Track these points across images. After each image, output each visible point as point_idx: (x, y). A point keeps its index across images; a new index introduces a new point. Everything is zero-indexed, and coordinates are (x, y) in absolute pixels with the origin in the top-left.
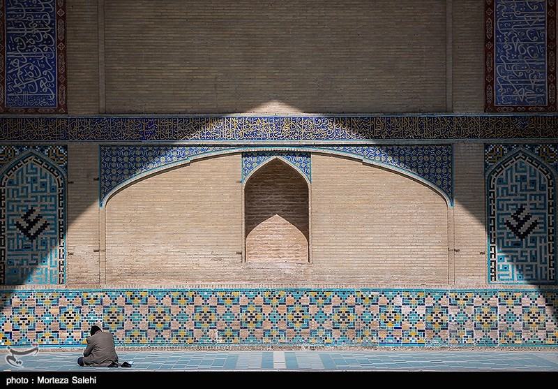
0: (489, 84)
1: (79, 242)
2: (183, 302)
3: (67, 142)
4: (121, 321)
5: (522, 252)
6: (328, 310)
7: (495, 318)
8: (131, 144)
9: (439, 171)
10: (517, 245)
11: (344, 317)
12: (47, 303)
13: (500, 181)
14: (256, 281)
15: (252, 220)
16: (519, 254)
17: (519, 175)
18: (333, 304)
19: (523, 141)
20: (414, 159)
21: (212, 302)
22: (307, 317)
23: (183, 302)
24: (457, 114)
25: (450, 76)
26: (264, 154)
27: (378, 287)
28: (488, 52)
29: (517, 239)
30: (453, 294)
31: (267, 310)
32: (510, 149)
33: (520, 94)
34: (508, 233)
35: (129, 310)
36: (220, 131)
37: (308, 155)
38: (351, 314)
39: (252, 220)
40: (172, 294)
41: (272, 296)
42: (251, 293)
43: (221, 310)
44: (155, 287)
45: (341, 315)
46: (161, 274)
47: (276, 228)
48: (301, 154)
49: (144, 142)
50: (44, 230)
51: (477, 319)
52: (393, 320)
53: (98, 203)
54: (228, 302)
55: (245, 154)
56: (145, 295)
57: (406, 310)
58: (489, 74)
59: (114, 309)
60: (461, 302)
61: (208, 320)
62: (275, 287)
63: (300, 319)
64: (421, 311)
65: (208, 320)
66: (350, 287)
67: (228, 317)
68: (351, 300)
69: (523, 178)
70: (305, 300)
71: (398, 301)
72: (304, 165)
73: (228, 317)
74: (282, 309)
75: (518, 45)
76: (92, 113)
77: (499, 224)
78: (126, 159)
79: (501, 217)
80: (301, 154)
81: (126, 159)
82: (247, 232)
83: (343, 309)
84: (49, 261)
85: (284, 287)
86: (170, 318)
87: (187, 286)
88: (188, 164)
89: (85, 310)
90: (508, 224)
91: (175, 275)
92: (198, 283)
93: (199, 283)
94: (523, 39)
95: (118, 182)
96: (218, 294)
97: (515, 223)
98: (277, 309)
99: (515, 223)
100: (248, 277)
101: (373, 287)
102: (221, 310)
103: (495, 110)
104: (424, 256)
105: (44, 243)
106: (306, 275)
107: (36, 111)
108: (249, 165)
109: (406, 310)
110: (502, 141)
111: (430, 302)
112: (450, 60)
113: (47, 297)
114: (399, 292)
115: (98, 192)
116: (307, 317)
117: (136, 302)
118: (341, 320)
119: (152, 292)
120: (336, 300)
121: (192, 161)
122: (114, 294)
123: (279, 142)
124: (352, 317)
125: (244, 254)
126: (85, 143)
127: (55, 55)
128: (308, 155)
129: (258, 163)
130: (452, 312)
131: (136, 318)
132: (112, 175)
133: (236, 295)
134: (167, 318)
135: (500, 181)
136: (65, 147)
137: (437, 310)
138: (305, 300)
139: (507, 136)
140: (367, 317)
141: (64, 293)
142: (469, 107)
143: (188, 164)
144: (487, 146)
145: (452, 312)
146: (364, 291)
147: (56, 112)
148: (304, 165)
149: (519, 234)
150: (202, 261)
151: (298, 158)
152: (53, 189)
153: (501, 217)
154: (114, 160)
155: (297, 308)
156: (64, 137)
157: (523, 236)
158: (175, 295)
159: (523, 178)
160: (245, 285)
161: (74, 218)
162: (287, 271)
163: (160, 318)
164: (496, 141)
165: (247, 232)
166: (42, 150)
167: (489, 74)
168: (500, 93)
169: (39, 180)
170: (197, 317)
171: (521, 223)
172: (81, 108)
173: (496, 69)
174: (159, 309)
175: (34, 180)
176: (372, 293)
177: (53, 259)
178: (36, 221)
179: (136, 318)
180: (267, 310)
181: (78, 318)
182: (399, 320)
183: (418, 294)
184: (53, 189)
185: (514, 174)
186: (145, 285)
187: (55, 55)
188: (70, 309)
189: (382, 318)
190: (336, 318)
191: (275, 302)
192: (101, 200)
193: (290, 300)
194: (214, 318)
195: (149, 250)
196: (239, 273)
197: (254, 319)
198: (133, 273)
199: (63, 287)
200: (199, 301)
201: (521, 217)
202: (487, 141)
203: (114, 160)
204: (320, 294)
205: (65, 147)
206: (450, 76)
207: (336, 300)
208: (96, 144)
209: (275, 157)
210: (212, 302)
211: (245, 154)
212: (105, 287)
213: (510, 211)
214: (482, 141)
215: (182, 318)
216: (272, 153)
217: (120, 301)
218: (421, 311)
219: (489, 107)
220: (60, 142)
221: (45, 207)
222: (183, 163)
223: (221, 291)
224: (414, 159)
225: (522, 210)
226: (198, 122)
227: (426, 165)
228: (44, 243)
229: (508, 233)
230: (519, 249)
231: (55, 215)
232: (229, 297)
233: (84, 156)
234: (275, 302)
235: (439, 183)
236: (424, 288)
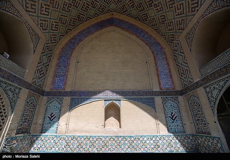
0: (160, 84)
1: (62, 121)
2: (87, 139)
3: (63, 97)
4: (69, 145)
5: (175, 124)
6: (126, 142)
7: (172, 143)
8: (78, 98)
9: (151, 104)
10: (173, 122)
11: (131, 144)
12: (51, 139)
13: (166, 106)
14: (107, 133)
15: (107, 117)
16: (174, 125)
17: (170, 104)
18: (128, 140)
19: (170, 96)
20: (145, 101)
21: (95, 140)
22: (121, 144)
23: (87, 139)
24: (154, 90)
25: (151, 83)
26: (109, 100)
27: (140, 135)
28: (158, 78)
29: (173, 121)
30: (160, 137)
31: (110, 142)
32: (167, 98)
33: (167, 86)
34: (170, 119)
35: (72, 142)
36: (101, 95)
37: (120, 100)
38: (133, 143)
39: (107, 117)
40: (84, 137)
41: (111, 138)
42: (105, 137)
43: (97, 142)
44: (80, 135)
45: (130, 143)
46: (82, 131)
47: (112, 120)
48: (118, 100)
49: (81, 97)
50: (53, 119)
51: (167, 144)
52: (144, 145)
53: (68, 112)
54: (99, 140)
55: (105, 100)
56: (77, 137)
57: (148, 142)
58: (159, 82)
59: (68, 141)
60: (162, 139)
61: (93, 145)
62: (112, 135)
63: (119, 145)
64: (152, 142)
65: (93, 145)
66: (132, 135)
67: (99, 144)
68: (133, 139)
69: (171, 105)
70: (120, 139)
71: (145, 139)
72: (119, 103)
73: (99, 144)
74: (114, 142)
75: (164, 76)
76: (70, 90)
77: (168, 117)
78: (76, 101)
79: (168, 115)
80: (118, 100)
81: (76, 101)
82: (105, 120)
83: (131, 142)
84: (54, 127)
85: (114, 135)
86: (83, 144)
87: (88, 135)
88: (91, 102)
89: (60, 141)
90: (170, 117)
91: (86, 132)
92: (92, 134)
93: (92, 134)
94: (165, 75)
95: (74, 107)
96: (96, 137)
97: (171, 117)
98: (112, 142)
99: (171, 117)
100: (105, 132)
101: (138, 135)
102: (97, 142)
103: (162, 90)
104: (150, 126)
105: (54, 122)
106: (120, 132)
107: (58, 90)
108: (106, 103)
109: (148, 142)
110: (165, 96)
111: (154, 139)
112: (151, 80)
113: (51, 137)
114: (145, 136)
115: (69, 109)
116: (121, 144)
117: (74, 139)
118: (130, 145)
119: (79, 136)
120: (129, 139)
121: (92, 102)
122: (69, 137)
123: (113, 97)
124: (133, 144)
125: (105, 126)
126: (67, 97)
127: (65, 78)
128: (120, 100)
129: (108, 102)
130: (160, 142)
131: (74, 144)
132: (72, 106)
133: (101, 137)
134: (82, 144)
135: (166, 106)
136: (63, 98)
137: (156, 142)
138: (120, 139)
139: (166, 95)
140: (137, 144)
141: (56, 136)
142: (157, 89)
143: (91, 102)
144: (162, 98)
145: (160, 142)
146: (136, 136)
147: (63, 90)
148: (119, 103)
149: (173, 119)
150: (93, 128)
151: (117, 101)
152: (59, 108)
153: (168, 115)
154: (74, 101)
155: (118, 141)
156: (63, 95)
157: (174, 120)
158: (85, 137)
159: (171, 105)
160: (104, 135)
161: (62, 115)
162: (115, 131)
163: (80, 144)
164: (164, 97)
165: (105, 120)
166: (58, 99)
167: (159, 82)
168: (162, 86)
169: (56, 106)
170: (91, 144)
171: (173, 117)
172: (68, 89)
173: (161, 81)
174: (80, 142)
175: (55, 106)
176: (138, 137)
177: (55, 126)
178: (53, 116)
179: (74, 144)
180: (110, 142)
181: (58, 144)
182: (146, 145)
183: (151, 137)
184: (59, 108)
185: (169, 104)
186: (77, 134)
187: (65, 78)
188: (56, 141)
189: (141, 144)
190: (129, 144)
191: (112, 140)
192: (69, 111)
193: (116, 139)
194: (95, 144)
195: (80, 124)
196: (103, 131)
197: (106, 145)
198: (75, 131)
199: (56, 134)
200: (91, 139)
201: (173, 115)
202: (162, 96)
203: (74, 101)
204: (124, 137)
205: (63, 98)
206: (151, 83)
207: (129, 139)
208: (70, 97)
209: (112, 101)
210: (95, 140)
211: (105, 100)
212: (67, 134)
213: (170, 113)
214: (161, 97)
215: (86, 144)
216: (111, 100)
217: (70, 139)
218: (152, 142)
219: (161, 89)
220: (62, 97)
221: (56, 113)
222: (90, 102)
223: (97, 136)
224: (145, 101)
225: (172, 113)
226: (95, 93)
227: (148, 102)
228: (54, 122)
229: (170, 119)
230: (174, 123)
231: (58, 115)
232: (99, 138)
233: (67, 100)
234: (112, 140)
235: (152, 107)
236: (152, 135)
